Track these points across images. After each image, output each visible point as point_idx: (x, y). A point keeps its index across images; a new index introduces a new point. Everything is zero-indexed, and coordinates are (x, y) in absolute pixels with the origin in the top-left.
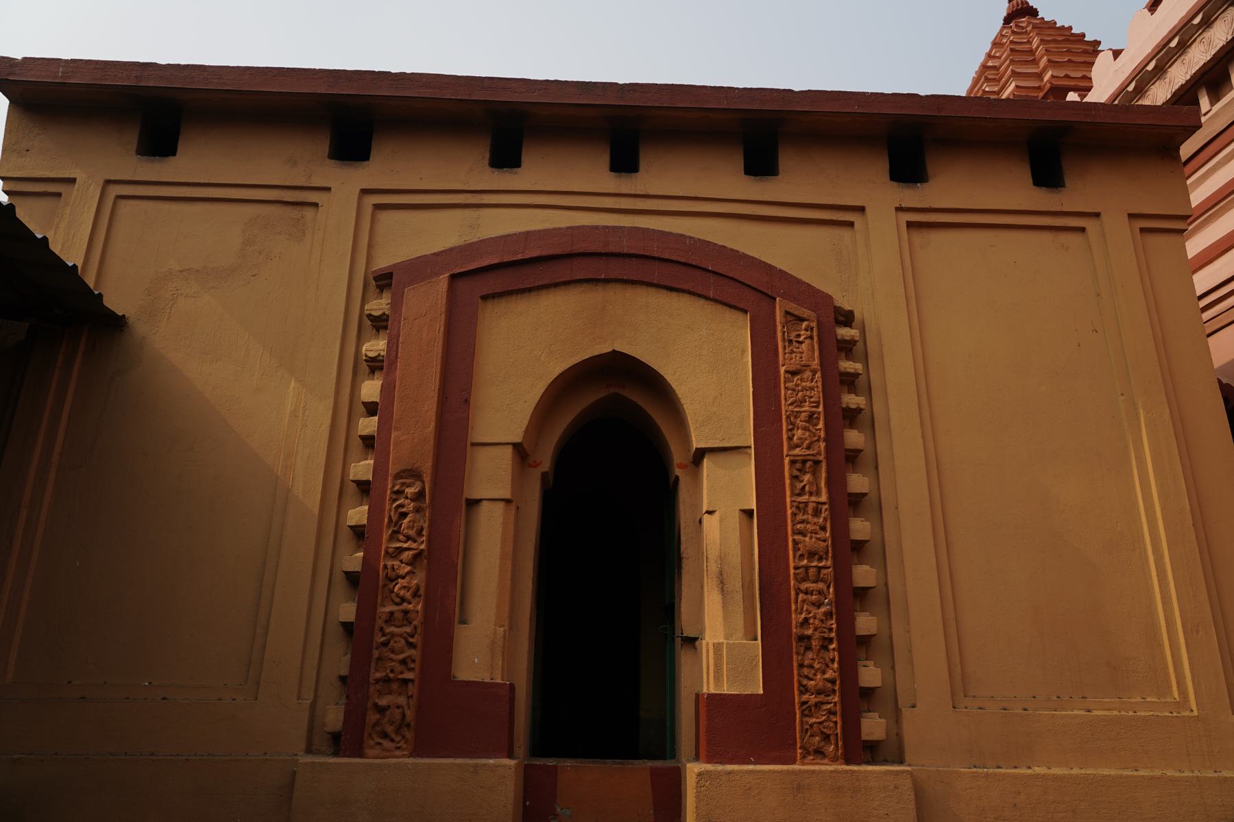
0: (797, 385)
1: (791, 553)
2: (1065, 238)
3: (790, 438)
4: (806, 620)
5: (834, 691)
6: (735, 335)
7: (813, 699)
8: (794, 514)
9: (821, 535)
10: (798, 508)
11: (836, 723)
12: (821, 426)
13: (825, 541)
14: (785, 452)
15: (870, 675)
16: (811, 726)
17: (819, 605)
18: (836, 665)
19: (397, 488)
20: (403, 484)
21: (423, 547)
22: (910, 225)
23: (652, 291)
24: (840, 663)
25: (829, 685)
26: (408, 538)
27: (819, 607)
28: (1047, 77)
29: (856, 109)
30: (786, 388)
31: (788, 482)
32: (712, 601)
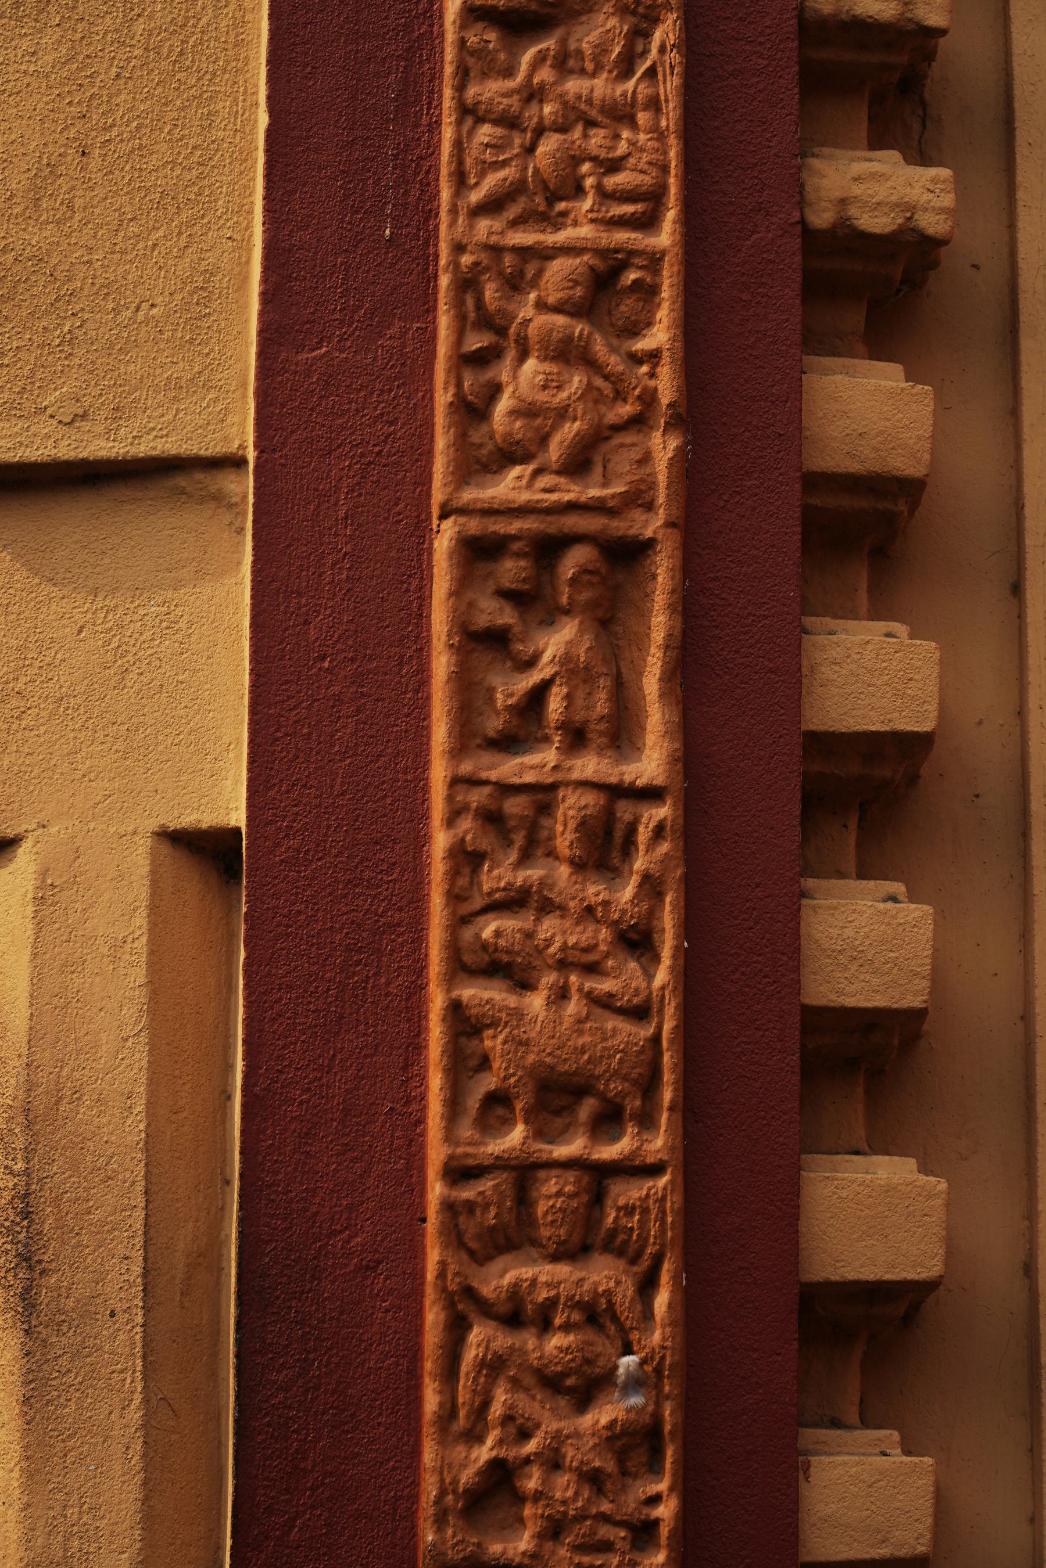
0: (533, 94)
1: (436, 1081)
3: (472, 411)
4: (501, 1475)
8: (466, 859)
9: (624, 978)
10: (492, 818)
12: (660, 335)
13: (640, 1013)
14: (438, 496)
17: (584, 1387)
30: (470, 113)
31: (441, 665)
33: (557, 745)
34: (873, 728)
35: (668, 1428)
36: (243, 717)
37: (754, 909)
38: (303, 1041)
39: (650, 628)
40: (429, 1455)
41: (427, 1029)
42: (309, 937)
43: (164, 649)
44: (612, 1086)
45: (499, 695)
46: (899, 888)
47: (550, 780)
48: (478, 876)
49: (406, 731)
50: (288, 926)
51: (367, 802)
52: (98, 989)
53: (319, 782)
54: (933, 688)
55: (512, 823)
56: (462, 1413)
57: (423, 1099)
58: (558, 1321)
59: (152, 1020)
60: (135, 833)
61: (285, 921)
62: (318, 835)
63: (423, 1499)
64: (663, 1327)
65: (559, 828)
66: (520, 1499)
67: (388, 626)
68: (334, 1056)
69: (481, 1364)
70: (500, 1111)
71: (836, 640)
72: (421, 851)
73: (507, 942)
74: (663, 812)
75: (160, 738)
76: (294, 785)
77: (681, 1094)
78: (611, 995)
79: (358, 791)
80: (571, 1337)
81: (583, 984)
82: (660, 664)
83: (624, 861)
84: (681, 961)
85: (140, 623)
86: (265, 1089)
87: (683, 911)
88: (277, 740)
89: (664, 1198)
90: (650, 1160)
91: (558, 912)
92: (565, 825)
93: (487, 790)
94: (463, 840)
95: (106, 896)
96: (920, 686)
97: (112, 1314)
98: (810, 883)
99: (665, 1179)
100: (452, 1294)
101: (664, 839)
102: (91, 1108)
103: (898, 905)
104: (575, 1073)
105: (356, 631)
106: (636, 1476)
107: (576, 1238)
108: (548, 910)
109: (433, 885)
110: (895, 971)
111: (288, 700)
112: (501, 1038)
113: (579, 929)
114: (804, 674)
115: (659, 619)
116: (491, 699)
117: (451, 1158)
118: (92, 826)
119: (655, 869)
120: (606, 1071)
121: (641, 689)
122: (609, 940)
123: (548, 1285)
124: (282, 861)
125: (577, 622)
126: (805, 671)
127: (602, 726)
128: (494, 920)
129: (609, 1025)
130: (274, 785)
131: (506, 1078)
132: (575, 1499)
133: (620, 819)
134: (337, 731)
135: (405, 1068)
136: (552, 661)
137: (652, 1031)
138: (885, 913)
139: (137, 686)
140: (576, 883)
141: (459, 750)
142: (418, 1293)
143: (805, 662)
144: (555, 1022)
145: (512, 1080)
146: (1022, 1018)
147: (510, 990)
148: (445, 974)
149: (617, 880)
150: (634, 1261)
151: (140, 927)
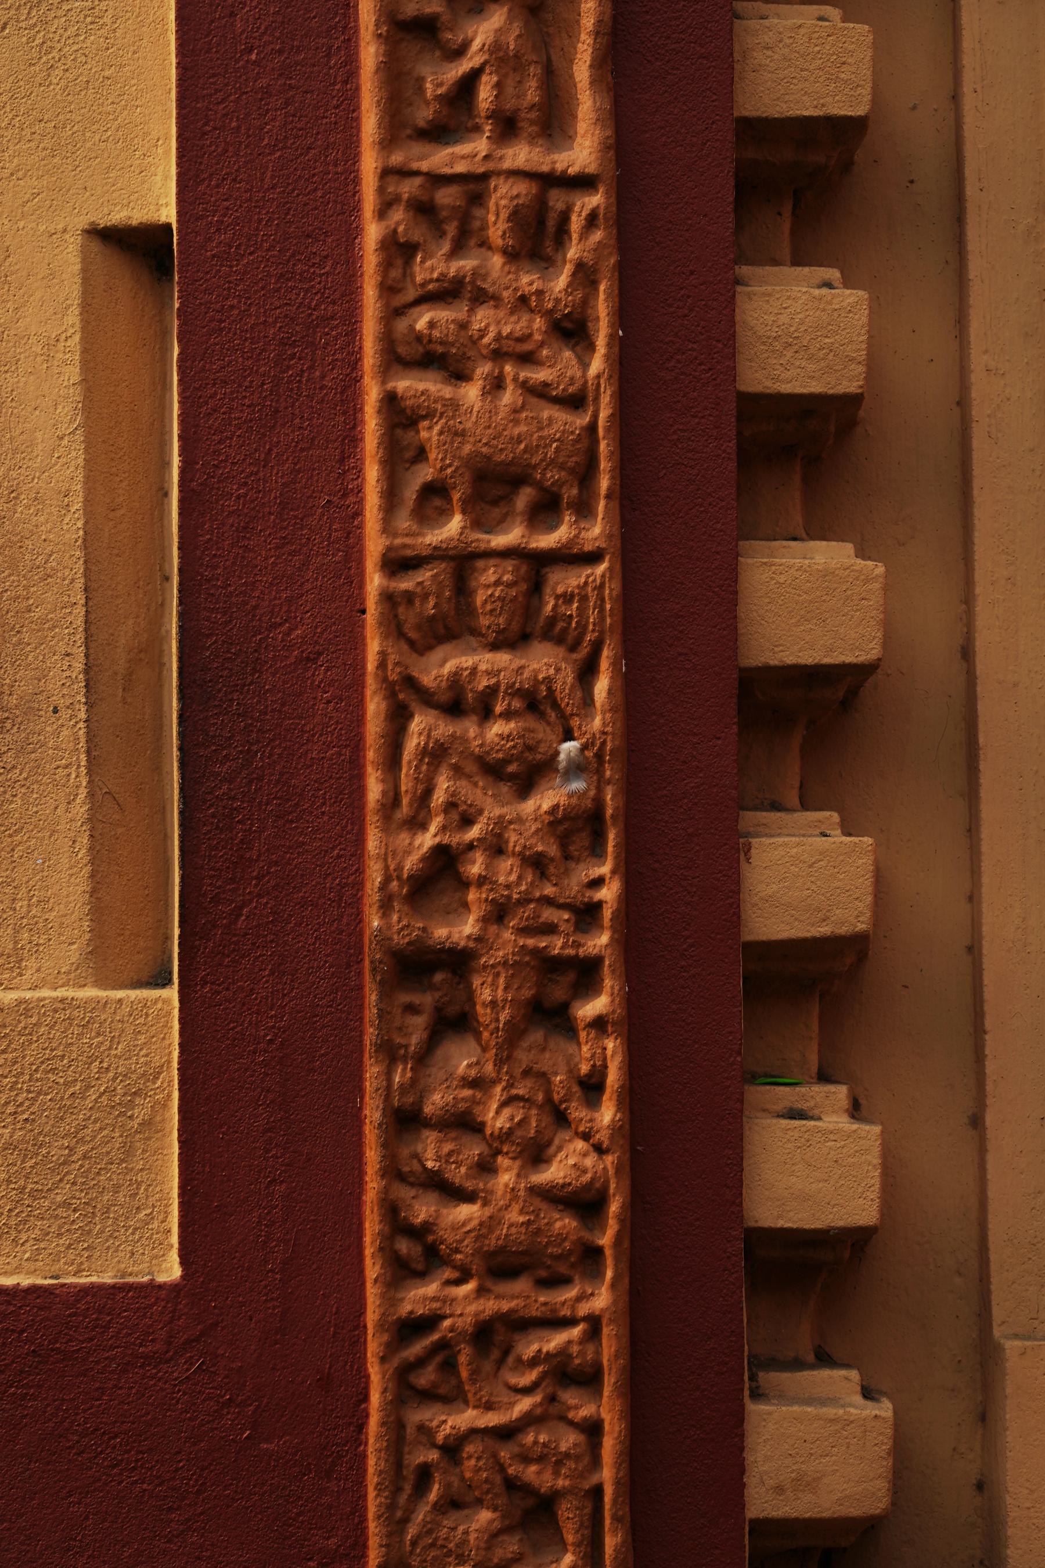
1: (372, 473)
4: (445, 862)
5: (592, 1255)
7: (466, 1303)
8: (399, 251)
9: (559, 367)
10: (424, 209)
11: (593, 1429)
13: (575, 401)
15: (813, 1162)
16: (452, 1450)
17: (526, 773)
18: (607, 1114)
24: (632, 1099)
25: (564, 1223)
27: (526, 784)
31: (369, 55)
33: (488, 134)
34: (806, 113)
35: (609, 811)
36: (171, 112)
37: (689, 297)
38: (239, 436)
39: (579, 15)
40: (373, 843)
41: (363, 422)
42: (242, 331)
43: (89, 45)
44: (548, 476)
45: (428, 85)
46: (833, 274)
47: (482, 170)
48: (411, 268)
49: (336, 123)
50: (221, 321)
51: (298, 195)
52: (32, 388)
53: (250, 175)
54: (866, 72)
55: (444, 214)
56: (405, 801)
57: (360, 491)
58: (498, 709)
59: (87, 418)
60: (65, 231)
61: (218, 316)
62: (249, 229)
63: (368, 885)
64: (603, 713)
65: (492, 218)
66: (465, 884)
67: (315, 17)
68: (270, 450)
69: (423, 752)
70: (437, 502)
71: (768, 25)
72: (353, 243)
73: (441, 333)
74: (595, 200)
75: (88, 135)
76: (224, 179)
77: (618, 482)
78: (546, 384)
79: (288, 184)
80: (512, 725)
81: (518, 374)
82: (590, 50)
83: (557, 250)
84: (616, 349)
85: (64, 19)
86: (201, 484)
87: (617, 300)
88: (206, 134)
89: (602, 586)
90: (588, 547)
91: (492, 303)
92: (498, 215)
93: (418, 181)
94: (395, 231)
95: (38, 295)
96: (853, 69)
97: (56, 711)
98: (745, 270)
99: (603, 567)
100: (393, 684)
101: (597, 227)
102: (28, 507)
103: (833, 291)
104: (512, 463)
105: (283, 22)
106: (578, 860)
107: (515, 626)
108: (481, 300)
109: (366, 278)
110: (831, 357)
111: (215, 94)
112: (437, 429)
113: (513, 319)
114: (736, 59)
115: (588, 5)
116: (420, 89)
117: (389, 549)
118: (21, 224)
119: (589, 258)
120: (542, 460)
121: (571, 76)
122: (543, 329)
123: (488, 673)
124: (214, 256)
125: (505, 9)
126: (737, 56)
127: (533, 115)
128: (428, 311)
129: (545, 414)
130: (204, 180)
131: (442, 469)
132: (518, 882)
133: (552, 208)
134: (266, 124)
135: (342, 460)
136: (481, 50)
137: (588, 419)
138: (820, 299)
139: (63, 83)
140: (509, 273)
141: (388, 141)
142: (358, 684)
143: (736, 47)
144: (490, 412)
145: (449, 471)
146: (958, 403)
147: (446, 381)
148: (380, 366)
149: (551, 269)
150: (573, 648)
151: (73, 326)
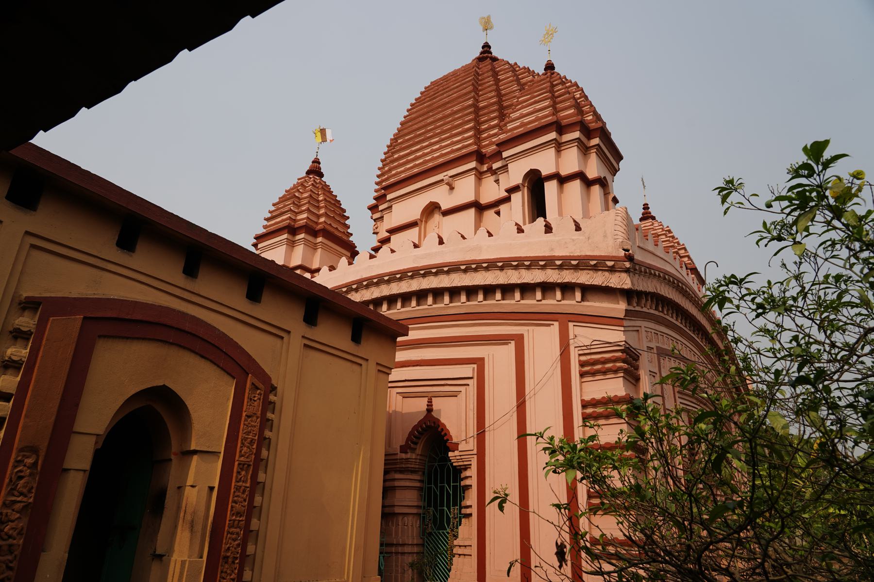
2: (355, 367)
3: (240, 452)
6: (226, 389)
12: (255, 446)
14: (237, 458)
17: (235, 540)
19: (19, 458)
20: (24, 456)
21: (31, 500)
22: (305, 345)
23: (193, 355)
26: (21, 494)
28: (322, 220)
29: (304, 287)
32: (183, 537)
